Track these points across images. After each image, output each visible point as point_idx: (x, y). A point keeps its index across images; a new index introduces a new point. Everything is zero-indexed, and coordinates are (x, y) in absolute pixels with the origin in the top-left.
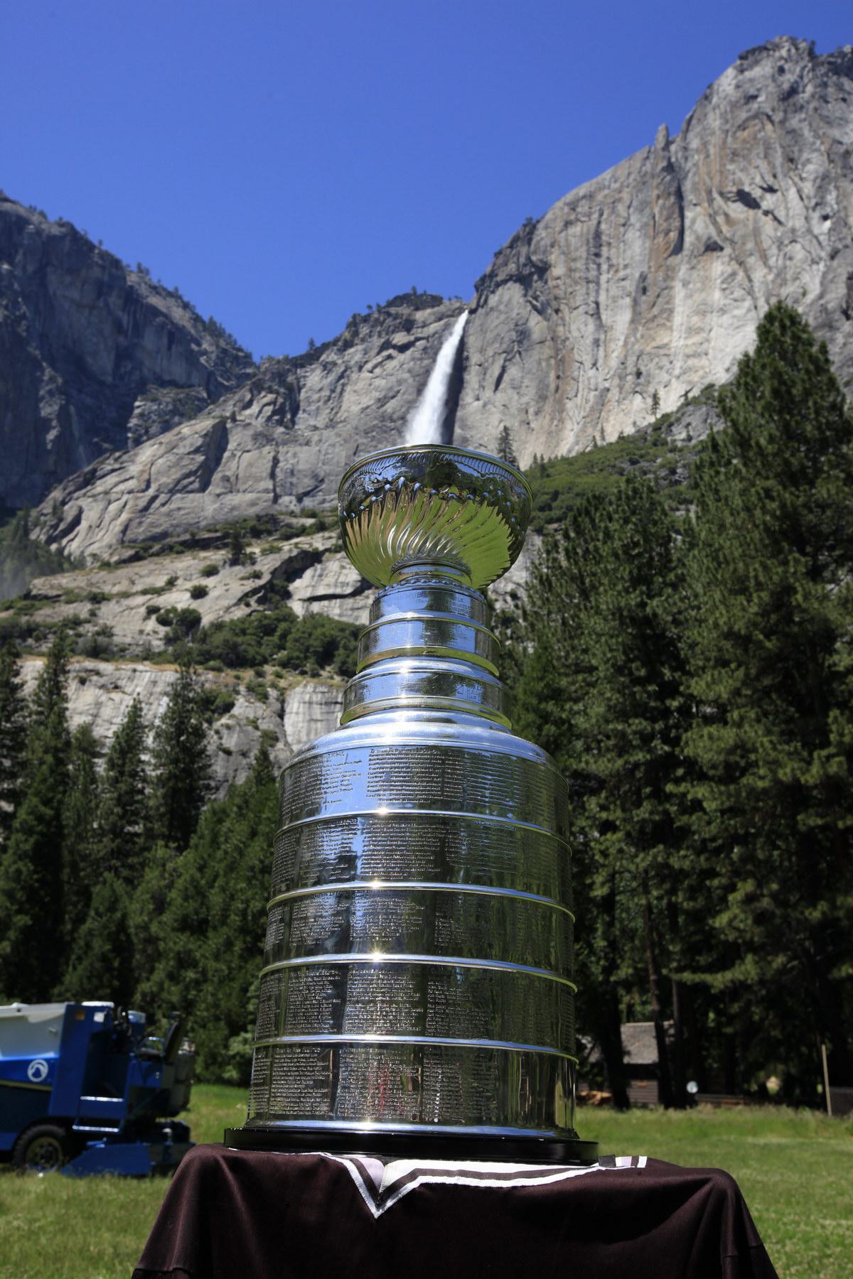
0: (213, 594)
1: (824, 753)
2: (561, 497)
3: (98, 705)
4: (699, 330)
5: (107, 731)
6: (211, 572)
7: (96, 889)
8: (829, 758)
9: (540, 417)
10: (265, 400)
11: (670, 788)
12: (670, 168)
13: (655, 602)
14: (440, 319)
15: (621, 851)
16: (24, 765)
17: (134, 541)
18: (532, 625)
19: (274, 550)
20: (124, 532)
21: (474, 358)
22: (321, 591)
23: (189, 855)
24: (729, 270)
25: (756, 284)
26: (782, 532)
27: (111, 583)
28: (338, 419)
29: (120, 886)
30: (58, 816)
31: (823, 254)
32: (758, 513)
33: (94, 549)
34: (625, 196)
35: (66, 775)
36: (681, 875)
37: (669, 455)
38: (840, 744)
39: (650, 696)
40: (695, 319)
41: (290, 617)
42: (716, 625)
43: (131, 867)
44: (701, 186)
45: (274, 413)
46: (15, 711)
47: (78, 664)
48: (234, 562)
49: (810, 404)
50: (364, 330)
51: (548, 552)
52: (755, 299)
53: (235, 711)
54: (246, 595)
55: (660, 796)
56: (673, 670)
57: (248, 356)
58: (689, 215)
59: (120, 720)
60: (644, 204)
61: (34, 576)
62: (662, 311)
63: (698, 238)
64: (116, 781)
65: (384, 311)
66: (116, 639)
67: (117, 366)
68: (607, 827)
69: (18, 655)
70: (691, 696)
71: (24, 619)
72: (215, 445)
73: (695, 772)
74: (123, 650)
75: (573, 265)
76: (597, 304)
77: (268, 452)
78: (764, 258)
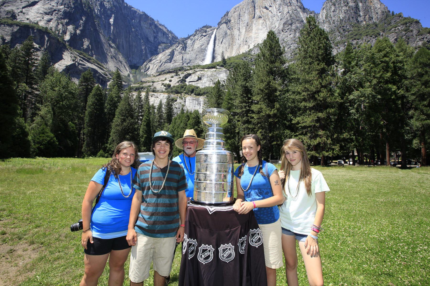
0: (173, 81)
3: (155, 100)
5: (156, 104)
6: (172, 77)
8: (274, 110)
11: (249, 115)
12: (253, 2)
13: (248, 84)
16: (143, 111)
19: (183, 73)
20: (157, 70)
21: (217, 38)
22: (191, 80)
23: (171, 125)
25: (267, 25)
26: (269, 72)
27: (156, 79)
32: (265, 68)
34: (245, 7)
36: (250, 128)
40: (256, 31)
41: (186, 85)
42: (258, 88)
43: (162, 127)
45: (182, 48)
47: (151, 93)
48: (176, 75)
50: (198, 32)
52: (267, 27)
53: (177, 101)
55: (247, 116)
56: (250, 95)
57: (177, 37)
58: (256, 11)
60: (248, 9)
62: (251, 29)
63: (257, 16)
65: (201, 29)
67: (154, 39)
68: (238, 121)
69: (141, 92)
70: (252, 100)
71: (141, 86)
72: (172, 54)
73: (253, 112)
77: (181, 55)
78: (269, 20)
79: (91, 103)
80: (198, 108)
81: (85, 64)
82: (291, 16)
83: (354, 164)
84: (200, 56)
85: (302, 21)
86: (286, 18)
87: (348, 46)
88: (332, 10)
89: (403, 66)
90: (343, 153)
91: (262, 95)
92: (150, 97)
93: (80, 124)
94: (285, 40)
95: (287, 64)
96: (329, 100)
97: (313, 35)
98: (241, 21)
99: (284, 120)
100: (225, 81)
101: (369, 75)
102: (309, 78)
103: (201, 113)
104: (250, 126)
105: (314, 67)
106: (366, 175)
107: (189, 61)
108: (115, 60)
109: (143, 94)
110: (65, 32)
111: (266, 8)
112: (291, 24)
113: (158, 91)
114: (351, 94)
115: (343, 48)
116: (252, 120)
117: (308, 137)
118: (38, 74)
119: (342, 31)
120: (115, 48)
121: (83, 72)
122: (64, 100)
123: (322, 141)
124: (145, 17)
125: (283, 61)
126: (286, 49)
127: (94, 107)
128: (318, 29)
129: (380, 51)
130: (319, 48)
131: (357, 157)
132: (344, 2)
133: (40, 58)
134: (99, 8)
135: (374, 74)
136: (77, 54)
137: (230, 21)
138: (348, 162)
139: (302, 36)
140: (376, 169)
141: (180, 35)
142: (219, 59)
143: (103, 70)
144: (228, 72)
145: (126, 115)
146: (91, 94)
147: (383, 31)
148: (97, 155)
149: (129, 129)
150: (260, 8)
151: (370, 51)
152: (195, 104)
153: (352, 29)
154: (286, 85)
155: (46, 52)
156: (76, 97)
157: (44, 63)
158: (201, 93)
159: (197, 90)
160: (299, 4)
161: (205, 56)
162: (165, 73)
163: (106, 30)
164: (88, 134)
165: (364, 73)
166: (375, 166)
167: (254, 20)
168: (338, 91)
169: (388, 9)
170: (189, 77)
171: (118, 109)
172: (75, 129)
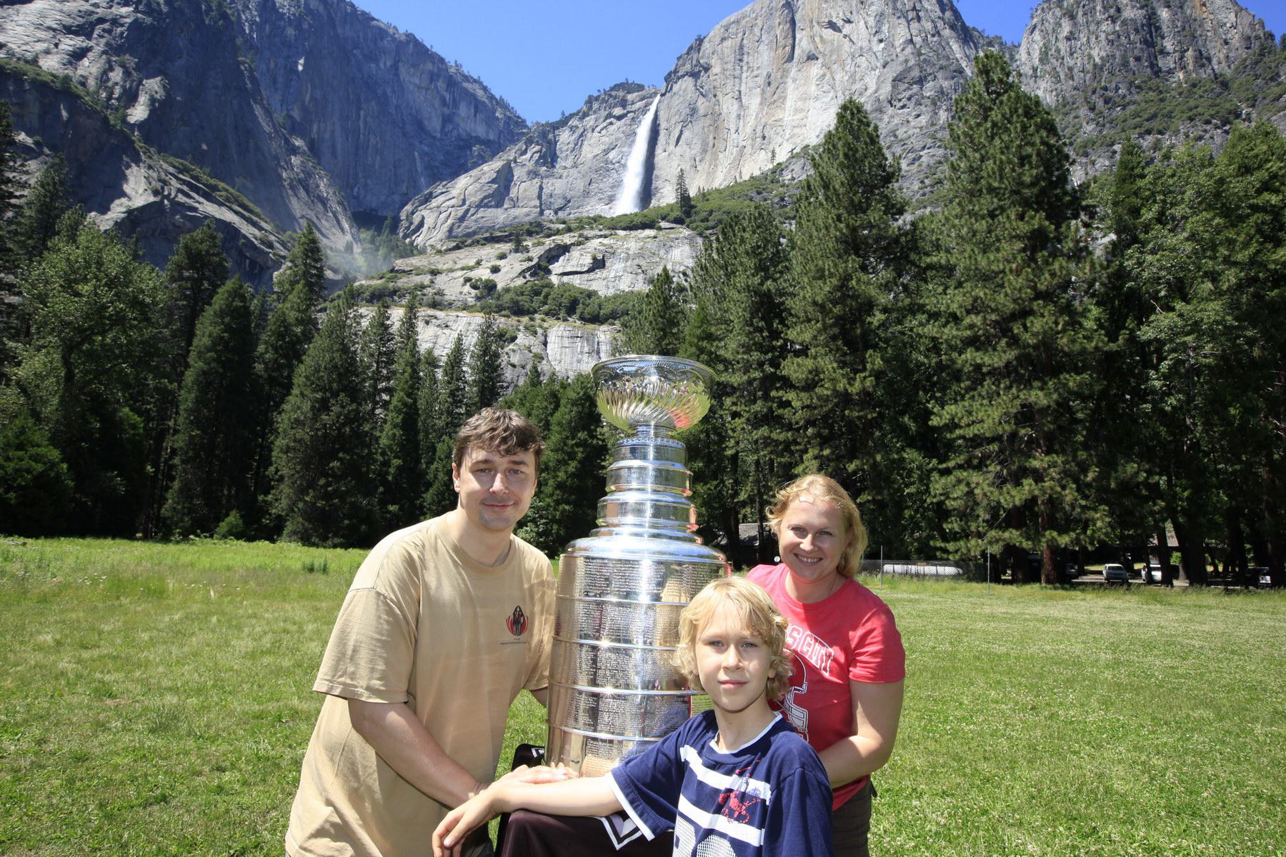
0: (503, 270)
1: (863, 375)
2: (714, 214)
3: (437, 336)
4: (802, 110)
5: (443, 352)
6: (502, 257)
7: (439, 446)
9: (703, 164)
11: (773, 393)
12: (788, 5)
13: (769, 282)
14: (642, 99)
15: (743, 429)
16: (394, 373)
17: (456, 237)
18: (695, 294)
20: (450, 230)
21: (663, 125)
22: (569, 269)
24: (821, 72)
25: (837, 82)
27: (443, 263)
28: (579, 162)
30: (415, 401)
32: (832, 230)
33: (431, 242)
34: (759, 22)
35: (420, 378)
36: (777, 443)
37: (780, 189)
38: (872, 370)
39: (764, 338)
41: (550, 285)
42: (804, 298)
44: (807, 19)
45: (540, 157)
46: (389, 341)
47: (424, 312)
48: (517, 251)
50: (595, 106)
51: (706, 250)
53: (517, 341)
55: (766, 397)
57: (524, 121)
58: (798, 36)
59: (451, 345)
61: (396, 258)
62: (780, 98)
63: (803, 51)
64: (449, 383)
66: (447, 298)
67: (443, 127)
68: (735, 415)
69: (388, 307)
70: (786, 340)
71: (391, 285)
72: (504, 179)
73: (787, 383)
74: (450, 304)
76: (740, 92)
77: (536, 182)
78: (843, 66)
79: (206, 341)
81: (196, 205)
82: (920, 54)
83: (1167, 581)
85: (960, 71)
86: (901, 58)
87: (1130, 151)
88: (1065, 34)
90: (1122, 538)
91: (819, 325)
92: (420, 326)
93: (163, 417)
94: (900, 133)
95: (908, 217)
96: (1063, 341)
97: (999, 116)
98: (745, 68)
99: (903, 413)
100: (689, 272)
101: (1208, 253)
102: (990, 263)
104: (779, 435)
105: (1007, 225)
106: (1222, 627)
108: (302, 193)
109: (397, 315)
110: (130, 97)
112: (921, 81)
114: (1142, 323)
115: (1107, 163)
116: (786, 412)
117: (991, 476)
118: (22, 234)
120: (304, 153)
121: (190, 231)
122: (111, 329)
123: (1043, 491)
124: (414, 51)
125: (893, 206)
128: (1018, 97)
129: (1246, 170)
130: (1024, 160)
132: (1104, 7)
133: (32, 181)
134: (258, 19)
136: (171, 170)
137: (707, 69)
138: (1143, 573)
139: (960, 119)
140: (1255, 600)
141: (533, 112)
142: (667, 197)
143: (261, 229)
144: (700, 240)
145: (331, 388)
146: (209, 312)
147: (1250, 102)
150: (812, 27)
152: (582, 353)
153: (1137, 98)
154: (906, 288)
155: (57, 161)
156: (155, 317)
157: (45, 196)
158: (602, 312)
160: (948, 14)
162: (478, 242)
163: (276, 90)
164: (187, 453)
165: (1188, 247)
166: (1251, 588)
167: (793, 68)
168: (1095, 311)
169: (1267, 29)
170: (561, 259)
171: (302, 367)
172: (139, 435)
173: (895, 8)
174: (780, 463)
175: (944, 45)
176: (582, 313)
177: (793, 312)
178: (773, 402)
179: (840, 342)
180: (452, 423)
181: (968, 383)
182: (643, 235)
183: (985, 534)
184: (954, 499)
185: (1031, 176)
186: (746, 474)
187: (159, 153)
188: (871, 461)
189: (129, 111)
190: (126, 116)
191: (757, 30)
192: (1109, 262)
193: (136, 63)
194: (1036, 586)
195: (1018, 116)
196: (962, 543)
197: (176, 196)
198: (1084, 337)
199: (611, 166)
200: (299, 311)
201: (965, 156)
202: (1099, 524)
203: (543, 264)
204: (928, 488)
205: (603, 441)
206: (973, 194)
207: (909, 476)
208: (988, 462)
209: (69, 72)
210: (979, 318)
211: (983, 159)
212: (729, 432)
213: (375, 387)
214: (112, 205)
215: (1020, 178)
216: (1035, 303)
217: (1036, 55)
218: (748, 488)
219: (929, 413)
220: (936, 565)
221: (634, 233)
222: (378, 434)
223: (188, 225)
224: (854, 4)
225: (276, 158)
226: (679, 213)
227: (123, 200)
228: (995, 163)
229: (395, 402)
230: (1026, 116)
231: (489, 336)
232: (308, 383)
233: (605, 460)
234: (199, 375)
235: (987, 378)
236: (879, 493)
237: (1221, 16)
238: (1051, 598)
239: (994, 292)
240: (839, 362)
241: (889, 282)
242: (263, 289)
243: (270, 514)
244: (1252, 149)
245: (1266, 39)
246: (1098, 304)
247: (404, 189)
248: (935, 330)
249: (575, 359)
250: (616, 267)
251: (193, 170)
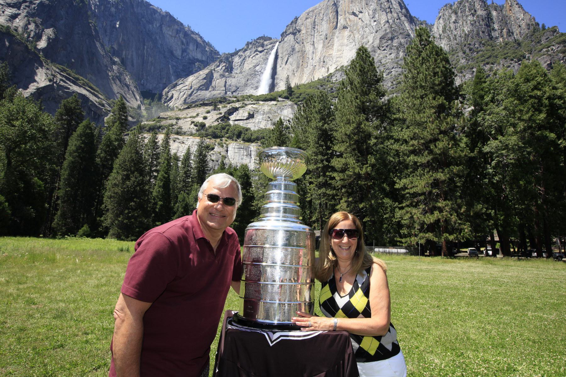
0: (209, 118)
1: (366, 166)
3: (178, 147)
5: (181, 154)
6: (208, 112)
7: (179, 196)
8: (367, 167)
10: (223, 65)
11: (327, 174)
12: (335, 4)
13: (326, 125)
14: (271, 44)
15: (314, 189)
16: (159, 163)
18: (294, 130)
19: (225, 107)
20: (185, 100)
21: (280, 55)
22: (238, 118)
27: (181, 114)
29: (186, 195)
30: (169, 176)
31: (374, 31)
32: (354, 103)
34: (322, 11)
35: (171, 166)
36: (329, 195)
40: (340, 47)
41: (229, 125)
42: (341, 132)
43: (188, 190)
45: (225, 69)
46: (157, 149)
47: (173, 136)
48: (215, 110)
49: (369, 74)
50: (250, 46)
51: (299, 111)
52: (355, 43)
53: (215, 150)
54: (218, 119)
55: (324, 175)
56: (330, 143)
57: (218, 52)
58: (339, 18)
62: (331, 45)
65: (256, 41)
66: (183, 130)
67: (182, 54)
68: (311, 183)
69: (157, 134)
70: (333, 151)
72: (209, 78)
73: (333, 169)
74: (185, 133)
75: (308, 30)
76: (314, 42)
77: (224, 79)
78: (359, 32)
79: (74, 148)
80: (248, 161)
81: (69, 86)
82: (391, 27)
83: (494, 255)
84: (253, 82)
86: (384, 29)
87: (480, 71)
88: (453, 20)
89: (563, 103)
90: (475, 237)
91: (348, 144)
92: (171, 142)
93: (53, 182)
94: (383, 61)
95: (386, 98)
96: (451, 152)
97: (425, 55)
98: (316, 31)
99: (383, 183)
100: (291, 120)
101: (512, 116)
102: (421, 118)
103: (252, 169)
105: (428, 102)
106: (516, 274)
107: (236, 88)
108: (118, 82)
109: (161, 137)
110: (38, 37)
111: (354, 14)
112: (392, 39)
113: (185, 133)
115: (470, 76)
116: (333, 182)
117: (421, 210)
119: (468, 51)
120: (119, 64)
121: (65, 99)
122: (29, 142)
123: (443, 216)
124: (169, 20)
125: (380, 93)
126: (384, 76)
127: (79, 155)
128: (433, 47)
129: (527, 80)
130: (435, 74)
131: (498, 244)
132: (469, 10)
134: (98, 3)
135: (519, 115)
136: (57, 70)
137: (299, 31)
138: (484, 252)
139: (409, 56)
141: (223, 49)
142: (281, 87)
143: (99, 98)
144: (296, 106)
145: (131, 170)
146: (75, 135)
147: (530, 52)
148: (78, 233)
149: (135, 191)
150: (345, 14)
151: (512, 80)
152: (243, 155)
153: (483, 49)
155: (4, 65)
156: (50, 137)
158: (252, 137)
159: (246, 132)
160: (404, 10)
161: (258, 82)
162: (197, 105)
163: (106, 36)
164: (64, 198)
165: (504, 113)
166: (529, 258)
168: (465, 140)
169: (536, 21)
170: (235, 113)
171: (118, 160)
172: (42, 190)
173: (381, 7)
174: (330, 204)
175: (402, 24)
176: (243, 138)
177: (336, 138)
178: (327, 177)
179: (356, 152)
180: (185, 185)
181: (411, 170)
182: (271, 104)
183: (418, 235)
184: (405, 220)
185: (438, 81)
186: (315, 209)
187: (52, 63)
188: (370, 203)
189: (38, 43)
190: (37, 45)
191: (321, 15)
192: (471, 118)
193: (41, 21)
194: (439, 258)
195: (433, 55)
196: (408, 239)
197: (60, 82)
198: (460, 151)
199: (257, 73)
200: (117, 135)
201: (411, 72)
202: (466, 230)
203: (227, 116)
204: (394, 215)
205: (253, 194)
206: (414, 88)
207: (386, 210)
208: (419, 204)
209: (10, 24)
210: (416, 141)
211: (418, 73)
212: (308, 190)
213: (151, 169)
214: (30, 86)
215: (434, 82)
216: (440, 136)
217: (441, 29)
218: (316, 215)
219: (395, 183)
220: (397, 249)
221: (267, 103)
222: (152, 190)
223: (65, 95)
224: (363, 5)
225: (106, 66)
226: (286, 94)
227: (35, 84)
228: (423, 75)
229: (160, 176)
230: (436, 55)
231: (202, 147)
232: (120, 167)
233: (253, 203)
234: (70, 163)
235: (419, 168)
236: (372, 217)
237: (518, 15)
238: (446, 262)
239: (423, 130)
240: (356, 160)
241: (378, 126)
242: (99, 125)
243: (102, 226)
244: (530, 72)
245: (536, 25)
246: (466, 136)
247: (165, 82)
248: (397, 146)
249: (240, 158)
250: (259, 117)
251: (68, 71)
